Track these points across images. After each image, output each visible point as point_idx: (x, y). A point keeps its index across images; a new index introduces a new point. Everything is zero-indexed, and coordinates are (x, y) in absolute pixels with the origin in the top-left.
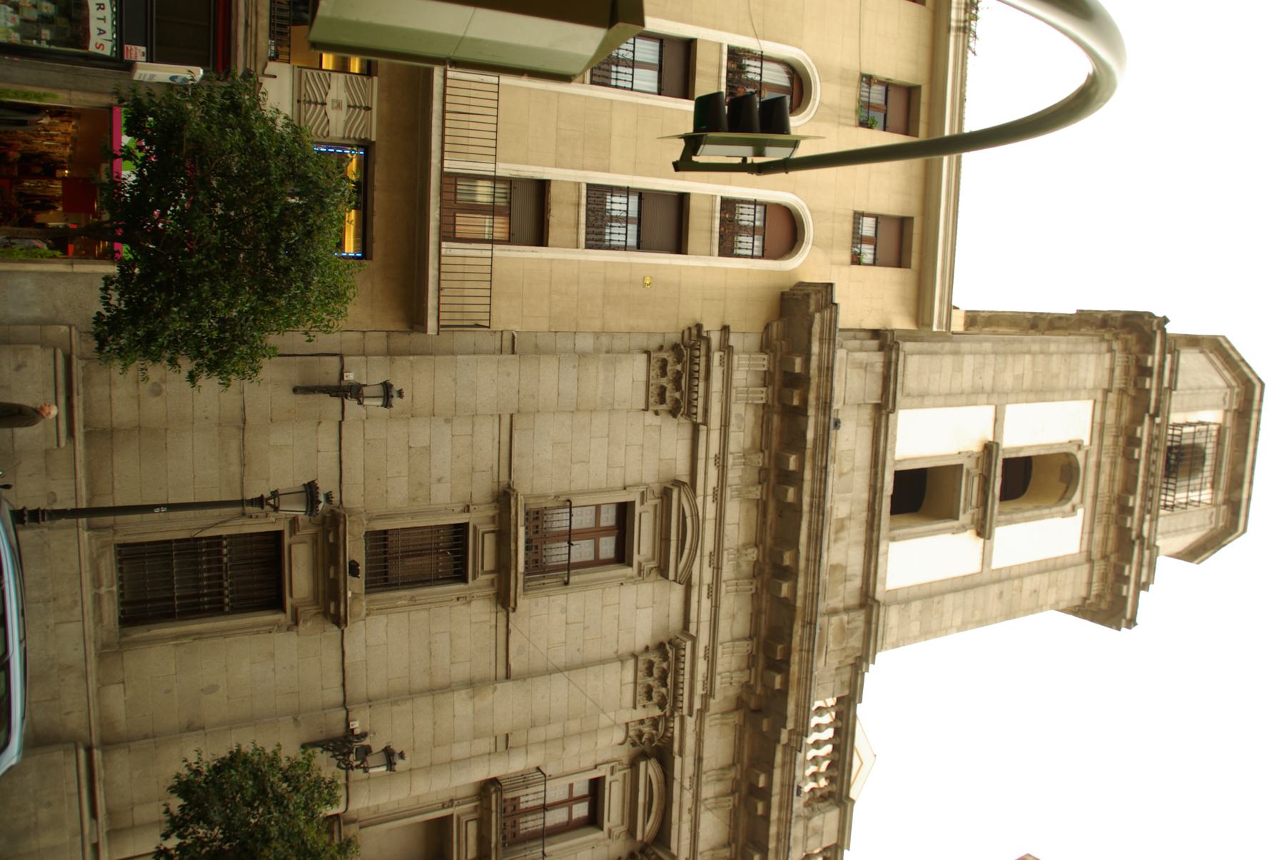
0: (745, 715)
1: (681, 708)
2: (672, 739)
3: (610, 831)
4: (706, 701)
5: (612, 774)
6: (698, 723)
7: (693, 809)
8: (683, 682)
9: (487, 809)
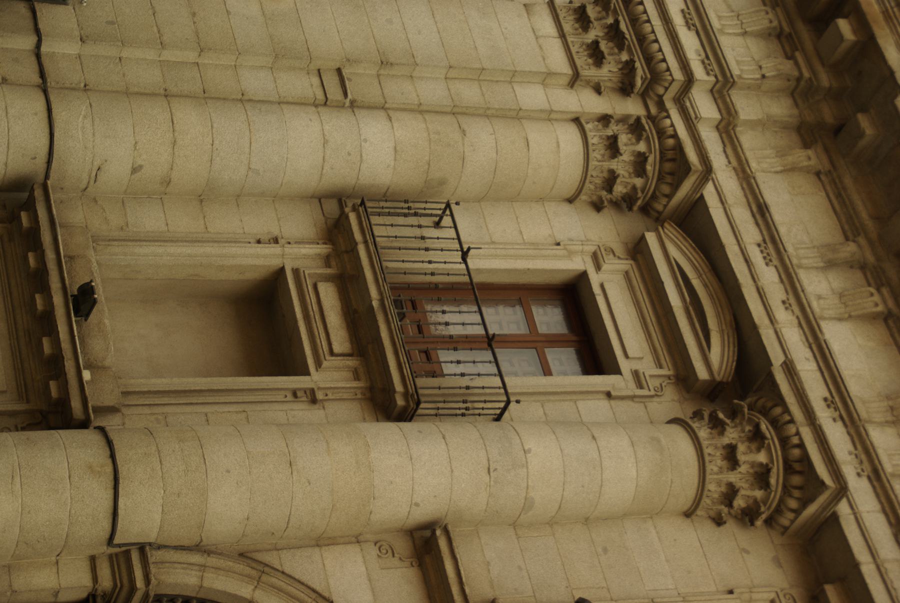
0: (827, 150)
1: (668, 69)
2: (679, 148)
3: (636, 374)
4: (725, 102)
5: (598, 267)
6: (729, 150)
7: (792, 300)
8: (653, 32)
9: (347, 252)
